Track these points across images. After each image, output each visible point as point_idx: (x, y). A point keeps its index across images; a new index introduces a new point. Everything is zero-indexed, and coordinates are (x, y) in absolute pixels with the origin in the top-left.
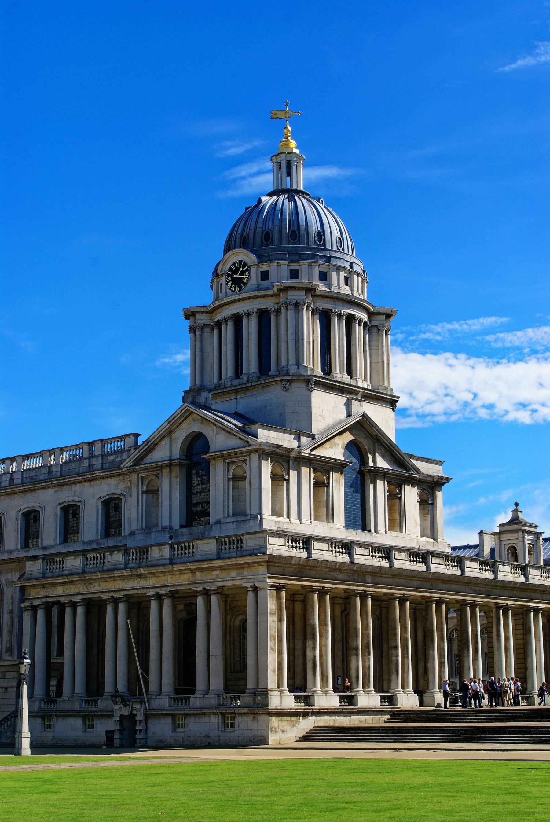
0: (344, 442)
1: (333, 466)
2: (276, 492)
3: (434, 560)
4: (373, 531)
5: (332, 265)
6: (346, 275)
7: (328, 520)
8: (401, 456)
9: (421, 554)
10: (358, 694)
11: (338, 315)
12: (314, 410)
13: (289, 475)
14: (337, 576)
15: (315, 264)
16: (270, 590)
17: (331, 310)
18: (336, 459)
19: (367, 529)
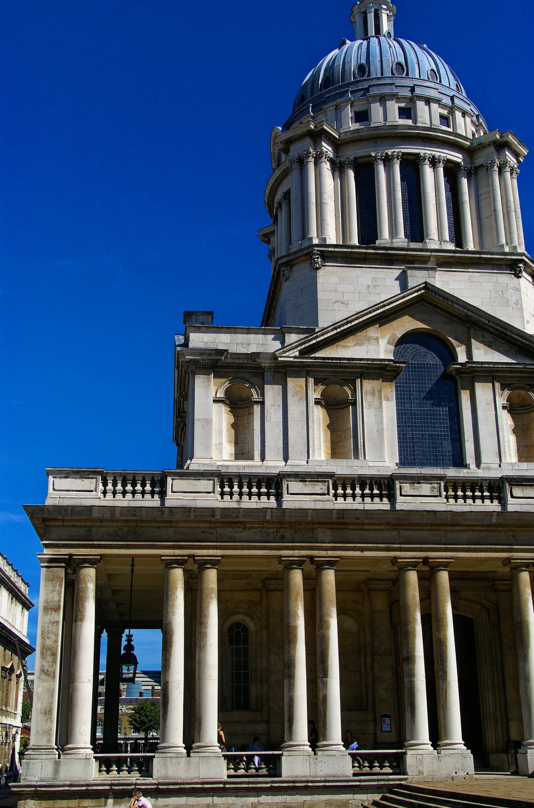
0: (394, 335)
1: (362, 372)
2: (247, 425)
3: (517, 491)
4: (473, 466)
5: (371, 96)
6: (403, 105)
7: (356, 456)
8: (526, 340)
9: (485, 484)
10: (285, 753)
11: (382, 159)
12: (321, 295)
13: (263, 395)
14: (234, 534)
15: (345, 104)
16: (47, 567)
17: (370, 156)
18: (361, 360)
19: (465, 465)
